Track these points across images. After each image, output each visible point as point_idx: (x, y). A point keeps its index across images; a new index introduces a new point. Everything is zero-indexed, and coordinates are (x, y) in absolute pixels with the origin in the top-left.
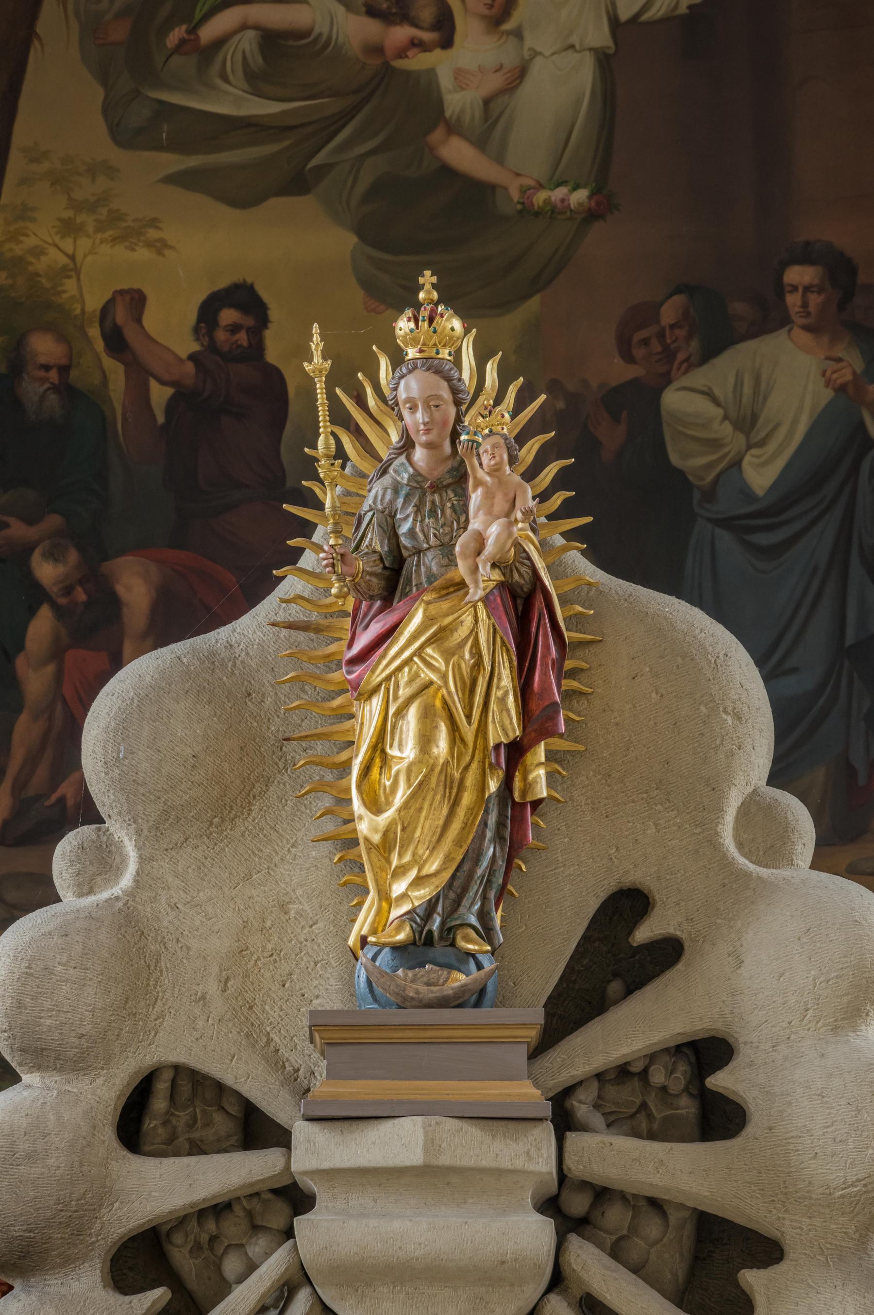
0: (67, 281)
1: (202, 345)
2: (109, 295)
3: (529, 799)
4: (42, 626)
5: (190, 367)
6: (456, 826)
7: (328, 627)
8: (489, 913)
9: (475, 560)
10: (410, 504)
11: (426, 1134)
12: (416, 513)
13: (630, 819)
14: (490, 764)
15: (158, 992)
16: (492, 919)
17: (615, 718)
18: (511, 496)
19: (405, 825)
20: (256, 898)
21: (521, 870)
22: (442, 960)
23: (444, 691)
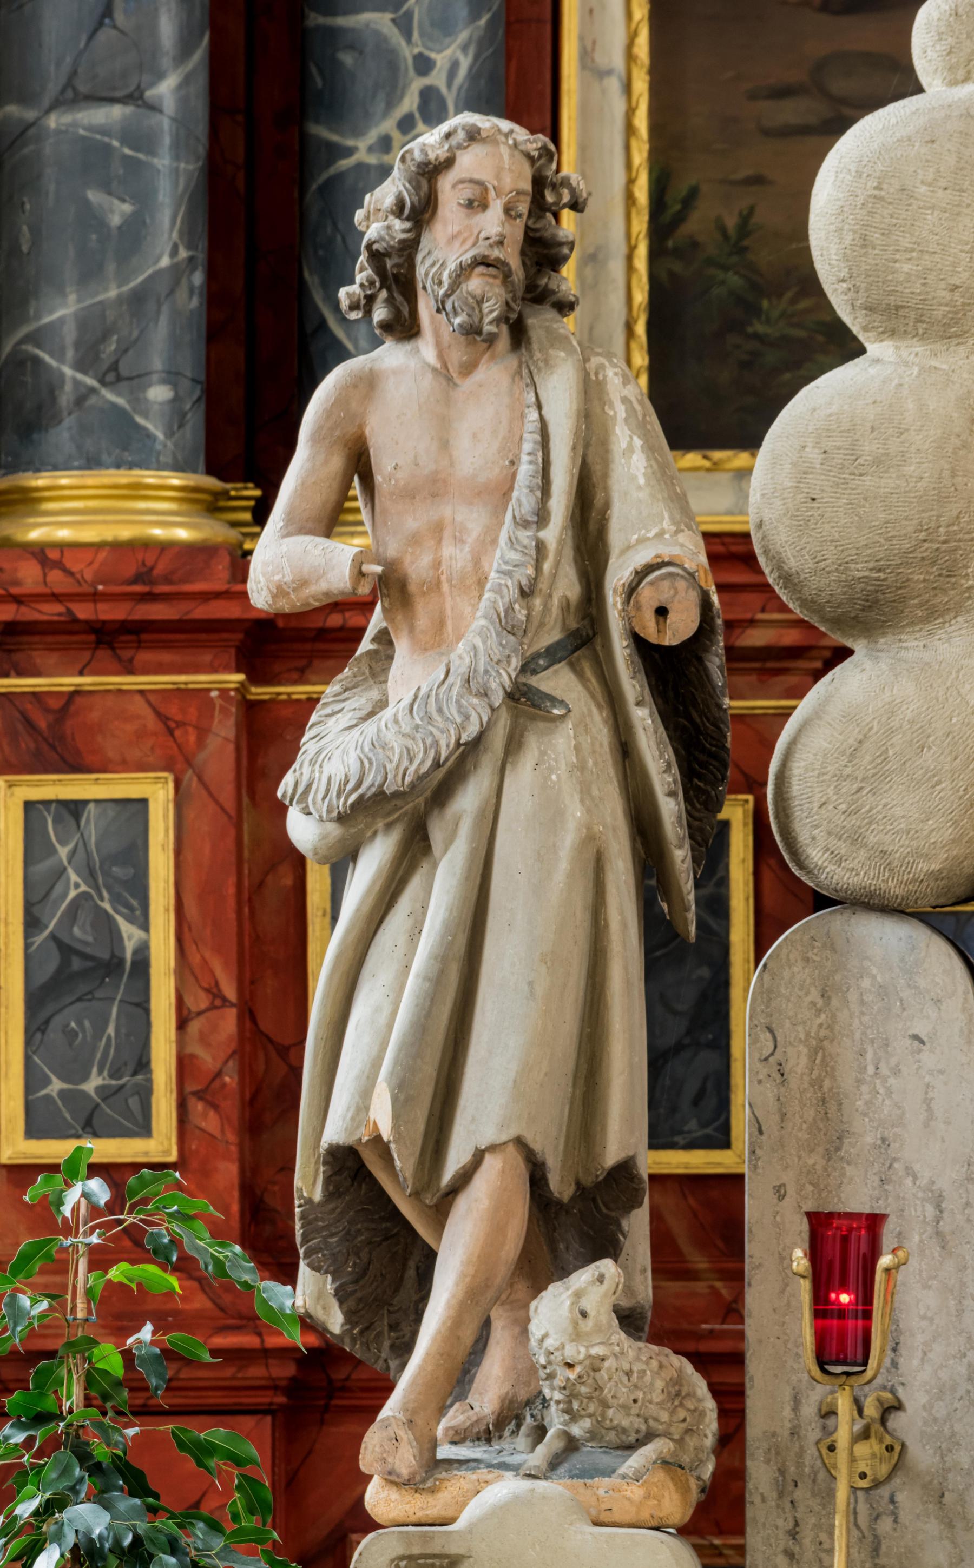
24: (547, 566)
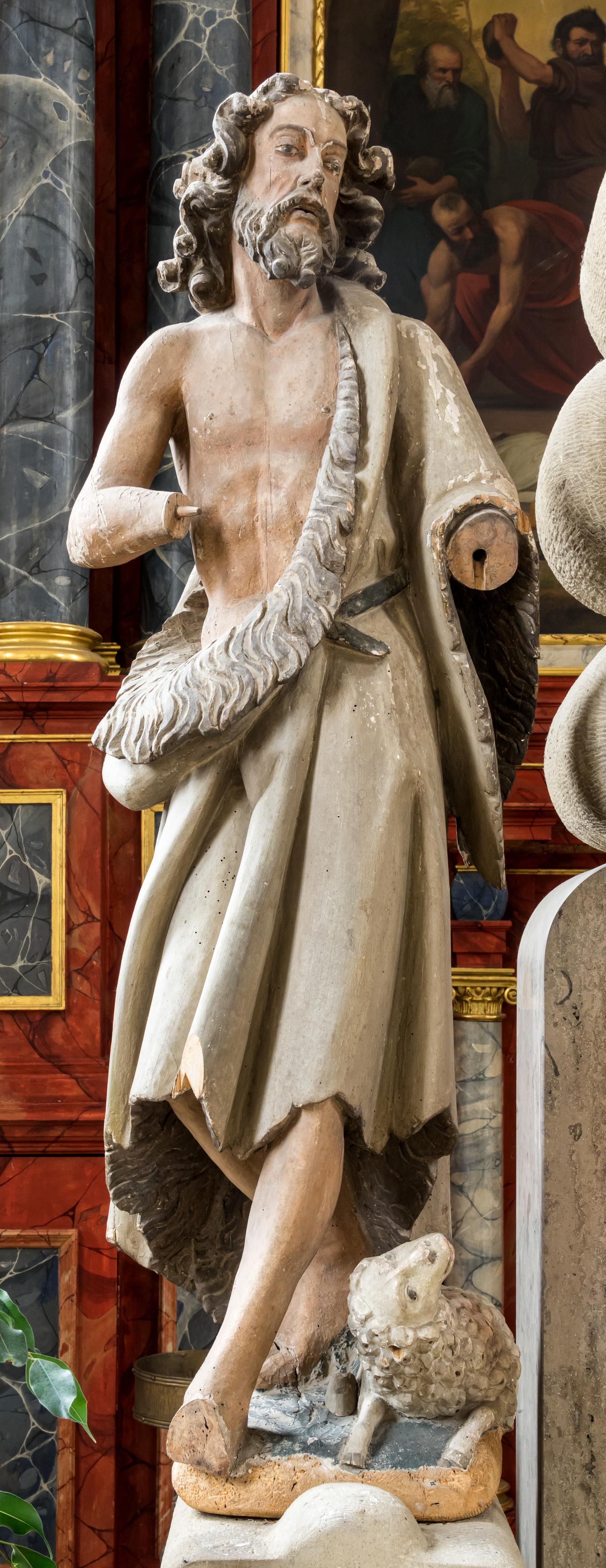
0: (458, 8)
1: (558, 54)
2: (489, 18)
4: (440, 257)
5: (549, 70)
24: (366, 506)
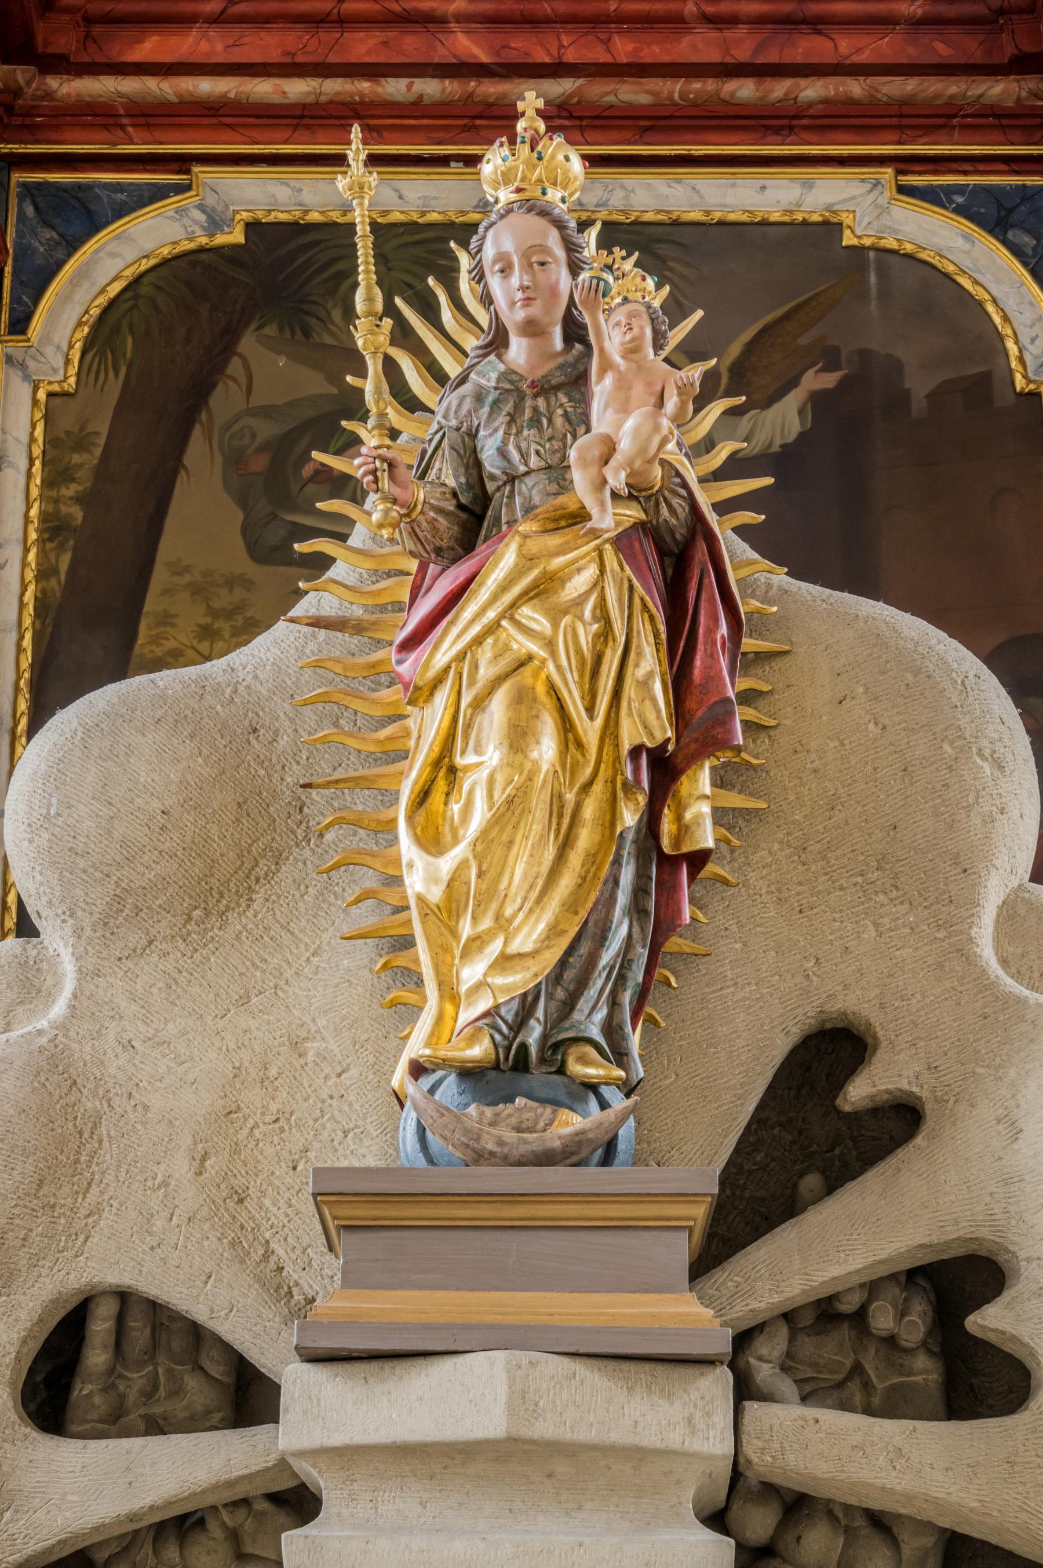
3: (685, 849)
6: (566, 882)
7: (374, 623)
8: (621, 1028)
9: (600, 470)
10: (499, 414)
11: (512, 1382)
12: (509, 424)
13: (837, 916)
14: (625, 784)
15: (93, 1174)
16: (624, 1038)
17: (813, 761)
18: (659, 388)
19: (484, 868)
20: (255, 1033)
21: (669, 985)
22: (543, 1093)
23: (551, 666)
